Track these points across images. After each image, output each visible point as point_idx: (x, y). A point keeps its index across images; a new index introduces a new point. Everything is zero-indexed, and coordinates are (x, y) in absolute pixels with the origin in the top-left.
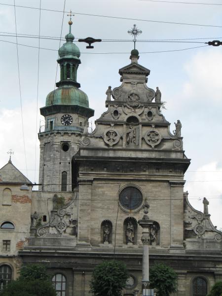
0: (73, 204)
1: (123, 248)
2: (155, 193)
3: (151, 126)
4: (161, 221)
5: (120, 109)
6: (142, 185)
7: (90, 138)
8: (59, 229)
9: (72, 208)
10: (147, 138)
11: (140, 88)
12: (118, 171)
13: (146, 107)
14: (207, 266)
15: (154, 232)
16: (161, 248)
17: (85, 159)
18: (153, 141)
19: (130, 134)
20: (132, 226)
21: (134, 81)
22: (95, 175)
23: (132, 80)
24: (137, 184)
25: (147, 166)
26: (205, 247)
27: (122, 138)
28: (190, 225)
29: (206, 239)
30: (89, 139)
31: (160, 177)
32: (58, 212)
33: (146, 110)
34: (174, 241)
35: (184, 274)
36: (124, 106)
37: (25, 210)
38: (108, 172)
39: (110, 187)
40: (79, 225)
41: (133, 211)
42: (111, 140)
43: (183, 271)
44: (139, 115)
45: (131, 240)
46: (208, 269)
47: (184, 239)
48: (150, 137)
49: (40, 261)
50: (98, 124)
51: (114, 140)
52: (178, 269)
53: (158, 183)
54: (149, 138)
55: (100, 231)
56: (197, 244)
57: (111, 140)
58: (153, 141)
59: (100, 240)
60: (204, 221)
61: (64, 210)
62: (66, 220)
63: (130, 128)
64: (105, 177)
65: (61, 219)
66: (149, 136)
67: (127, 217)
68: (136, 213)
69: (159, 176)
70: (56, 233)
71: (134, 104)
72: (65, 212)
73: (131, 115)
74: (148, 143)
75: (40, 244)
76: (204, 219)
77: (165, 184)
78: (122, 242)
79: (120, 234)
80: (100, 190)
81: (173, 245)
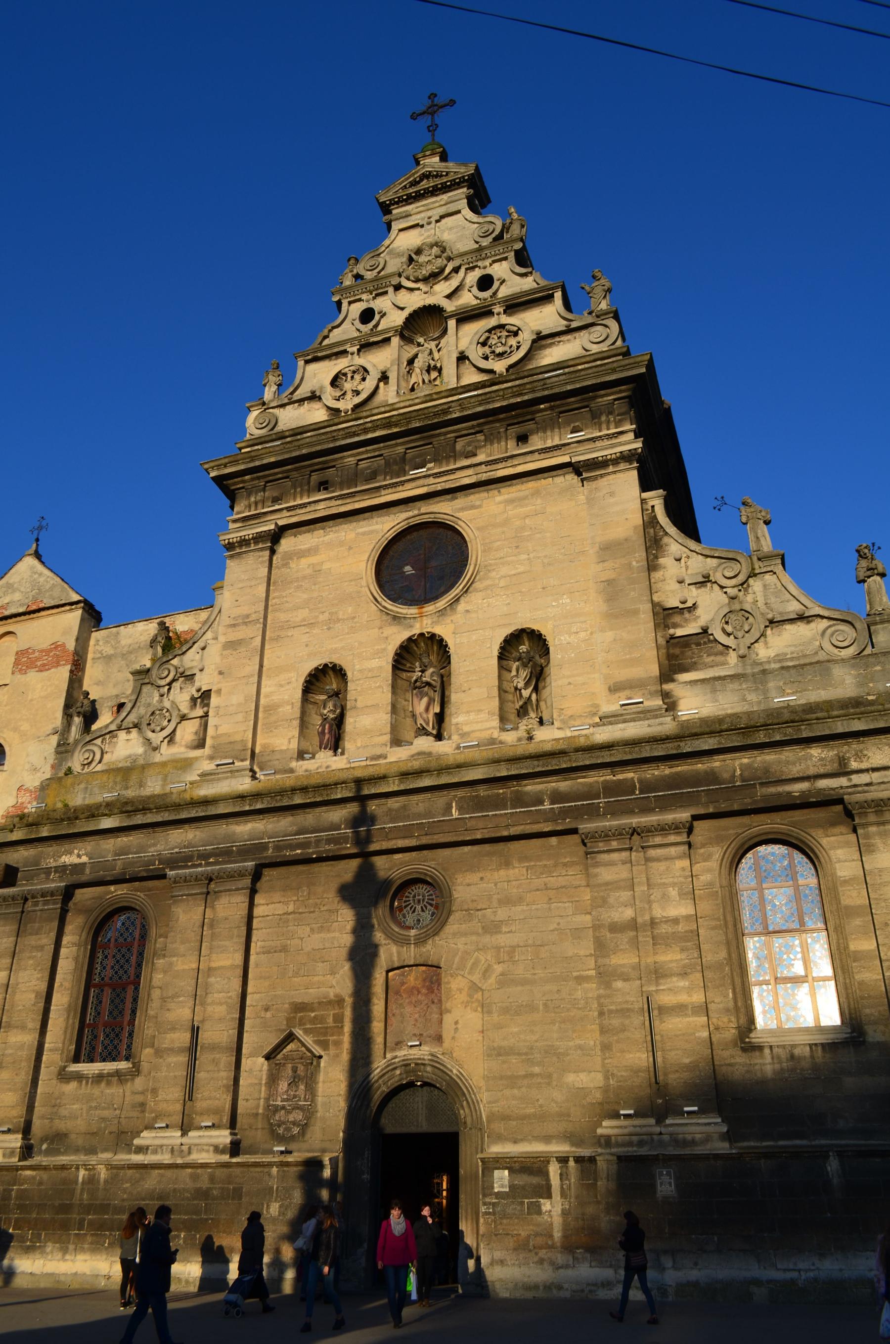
0: (209, 635)
1: (391, 759)
2: (518, 523)
3: (490, 313)
4: (550, 625)
5: (381, 304)
6: (462, 509)
7: (276, 411)
8: (150, 735)
9: (203, 649)
10: (475, 354)
11: (451, 229)
12: (373, 476)
13: (473, 268)
14: (795, 770)
15: (524, 674)
16: (559, 734)
17: (242, 467)
18: (501, 355)
19: (416, 360)
20: (431, 670)
21: (429, 213)
22: (285, 513)
23: (422, 215)
24: (442, 509)
25: (483, 438)
26: (773, 693)
27: (384, 377)
28: (687, 615)
29: (779, 658)
30: (272, 414)
31: (536, 456)
32: (154, 672)
33: (473, 277)
34: (615, 689)
35: (675, 827)
36: (398, 287)
37: (49, 690)
38: (333, 492)
39: (341, 543)
40: (214, 700)
41: (430, 608)
42: (349, 395)
43: (670, 817)
44: (449, 296)
45: (430, 729)
46: (804, 786)
47: (667, 674)
48: (490, 347)
49: (54, 865)
50: (307, 362)
51: (357, 393)
52: (646, 810)
53: (531, 485)
54: (481, 350)
55: (298, 715)
56: (735, 685)
57: (349, 395)
58: (501, 355)
59: (294, 745)
60: (756, 585)
61: (175, 662)
62: (181, 697)
63: (419, 345)
64: (322, 509)
65: (162, 696)
66: (484, 344)
67: (405, 635)
68: (442, 613)
69: (529, 458)
70: (140, 750)
71: (425, 272)
72: (176, 668)
73: (420, 304)
74: (483, 364)
75: (78, 799)
76: (753, 575)
77: (559, 480)
78: (387, 738)
79: (375, 706)
80: (304, 562)
81: (611, 706)
